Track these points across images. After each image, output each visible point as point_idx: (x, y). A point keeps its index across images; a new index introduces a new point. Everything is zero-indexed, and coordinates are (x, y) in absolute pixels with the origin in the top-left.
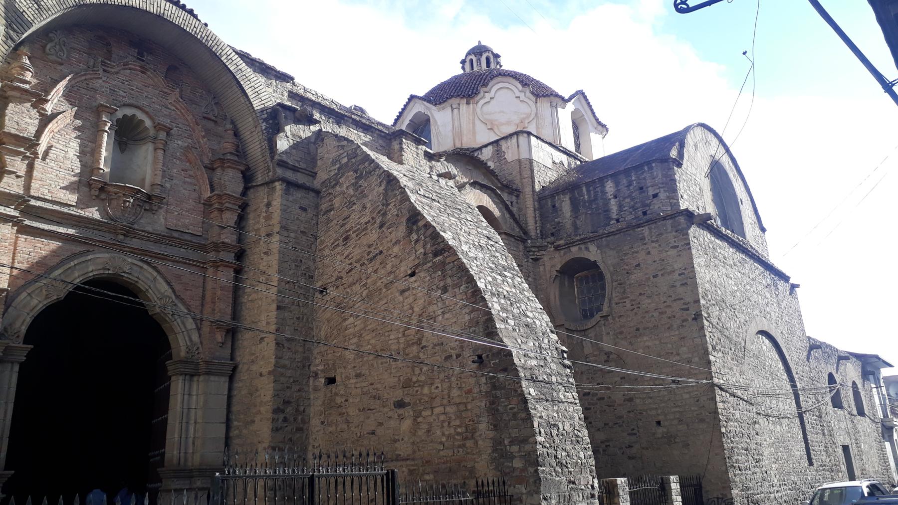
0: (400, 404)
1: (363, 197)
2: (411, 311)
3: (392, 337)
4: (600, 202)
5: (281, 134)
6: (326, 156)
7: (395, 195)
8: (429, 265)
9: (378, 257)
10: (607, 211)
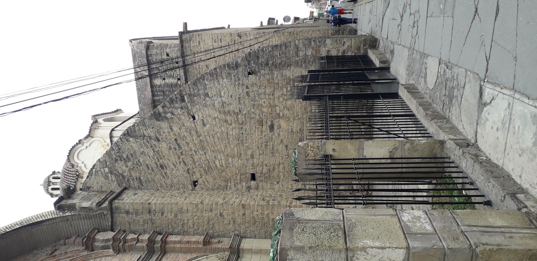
0: (272, 127)
3: (231, 133)
5: (77, 204)
8: (189, 105)
9: (179, 141)
10: (172, 85)
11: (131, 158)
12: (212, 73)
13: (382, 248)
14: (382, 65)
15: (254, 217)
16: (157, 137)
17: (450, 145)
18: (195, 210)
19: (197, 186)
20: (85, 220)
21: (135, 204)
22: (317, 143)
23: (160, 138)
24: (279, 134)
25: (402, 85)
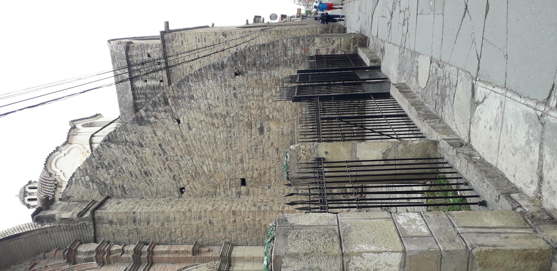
0: (261, 130)
3: (219, 137)
4: (148, 91)
5: (57, 216)
7: (121, 135)
8: (173, 108)
9: (164, 147)
10: (154, 87)
11: (113, 165)
12: (197, 74)
13: (378, 252)
14: (373, 64)
15: (245, 224)
16: (140, 143)
17: (443, 145)
18: (183, 218)
19: (184, 194)
20: (66, 232)
21: (119, 213)
22: (309, 146)
23: (143, 143)
24: (269, 137)
25: (394, 84)
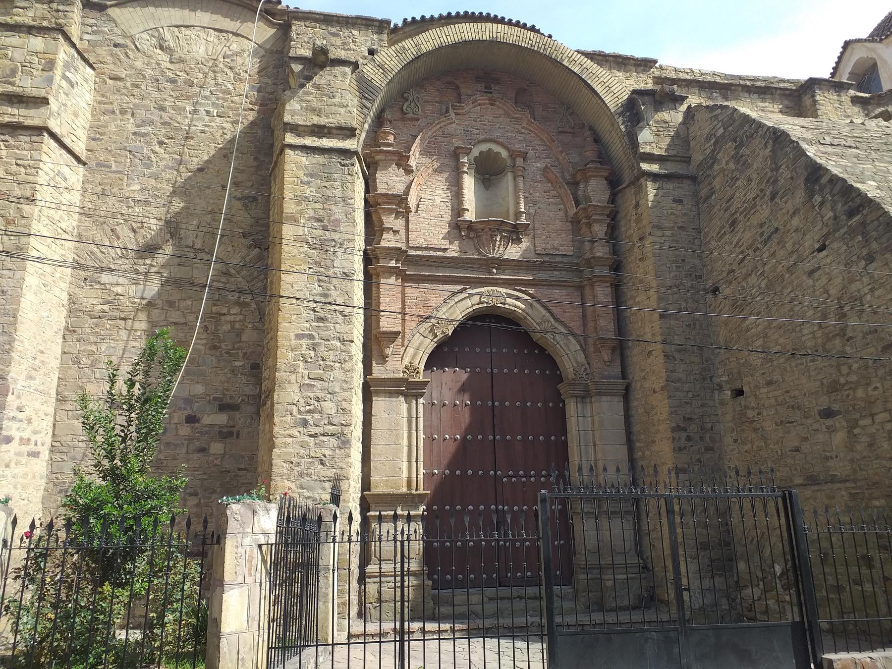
0: (828, 414)
1: (747, 168)
2: (825, 295)
3: (805, 332)
6: (698, 134)
7: (786, 154)
8: (843, 231)
9: (776, 238)
11: (741, 162)
15: (653, 408)
23: (776, 200)
24: (817, 430)
